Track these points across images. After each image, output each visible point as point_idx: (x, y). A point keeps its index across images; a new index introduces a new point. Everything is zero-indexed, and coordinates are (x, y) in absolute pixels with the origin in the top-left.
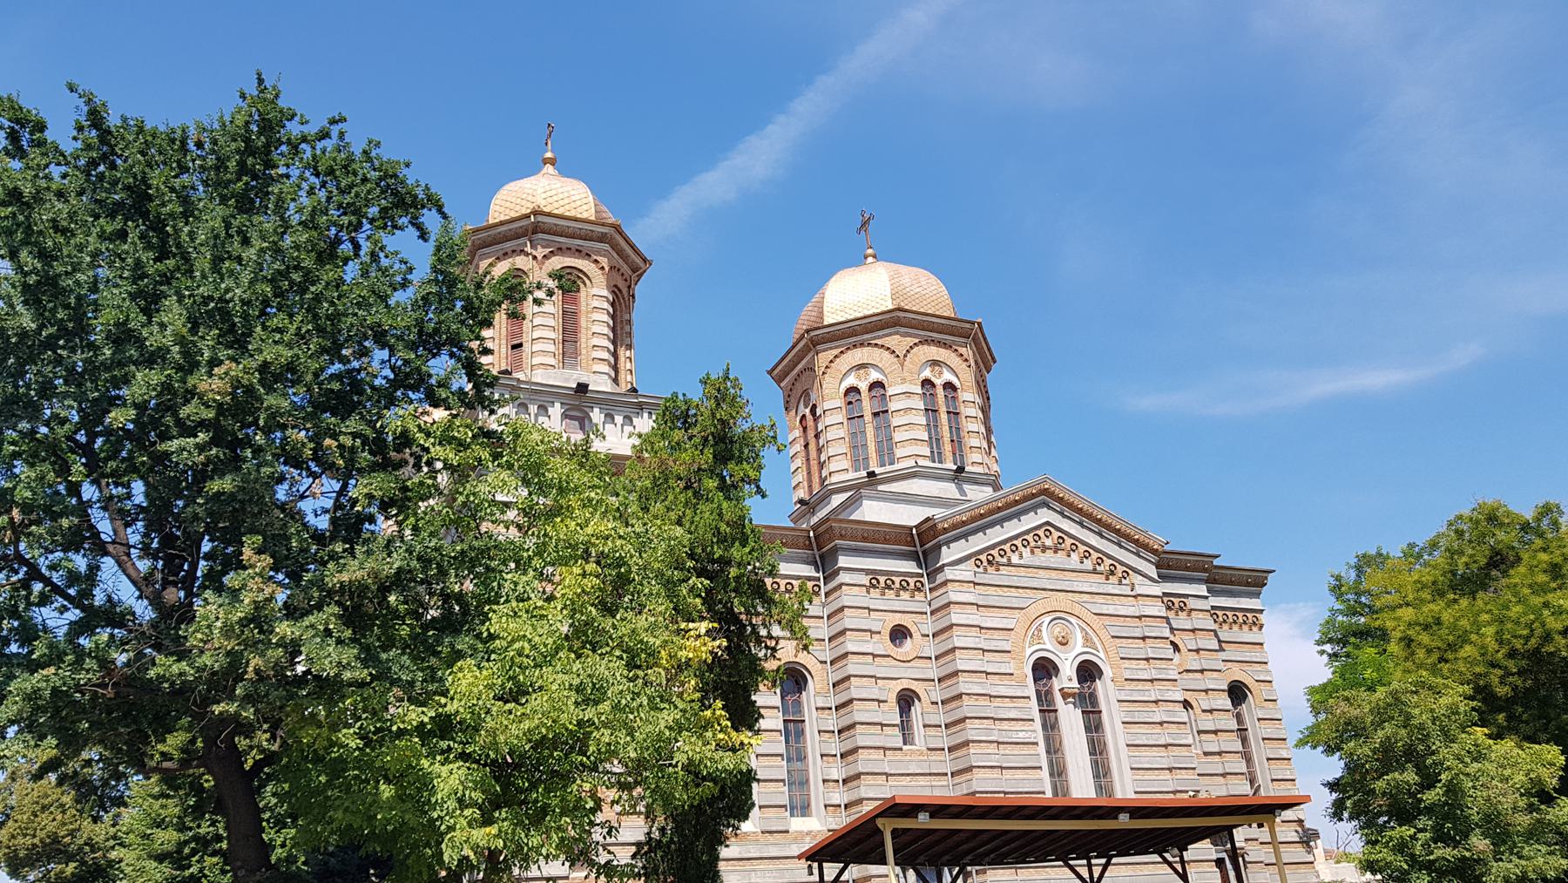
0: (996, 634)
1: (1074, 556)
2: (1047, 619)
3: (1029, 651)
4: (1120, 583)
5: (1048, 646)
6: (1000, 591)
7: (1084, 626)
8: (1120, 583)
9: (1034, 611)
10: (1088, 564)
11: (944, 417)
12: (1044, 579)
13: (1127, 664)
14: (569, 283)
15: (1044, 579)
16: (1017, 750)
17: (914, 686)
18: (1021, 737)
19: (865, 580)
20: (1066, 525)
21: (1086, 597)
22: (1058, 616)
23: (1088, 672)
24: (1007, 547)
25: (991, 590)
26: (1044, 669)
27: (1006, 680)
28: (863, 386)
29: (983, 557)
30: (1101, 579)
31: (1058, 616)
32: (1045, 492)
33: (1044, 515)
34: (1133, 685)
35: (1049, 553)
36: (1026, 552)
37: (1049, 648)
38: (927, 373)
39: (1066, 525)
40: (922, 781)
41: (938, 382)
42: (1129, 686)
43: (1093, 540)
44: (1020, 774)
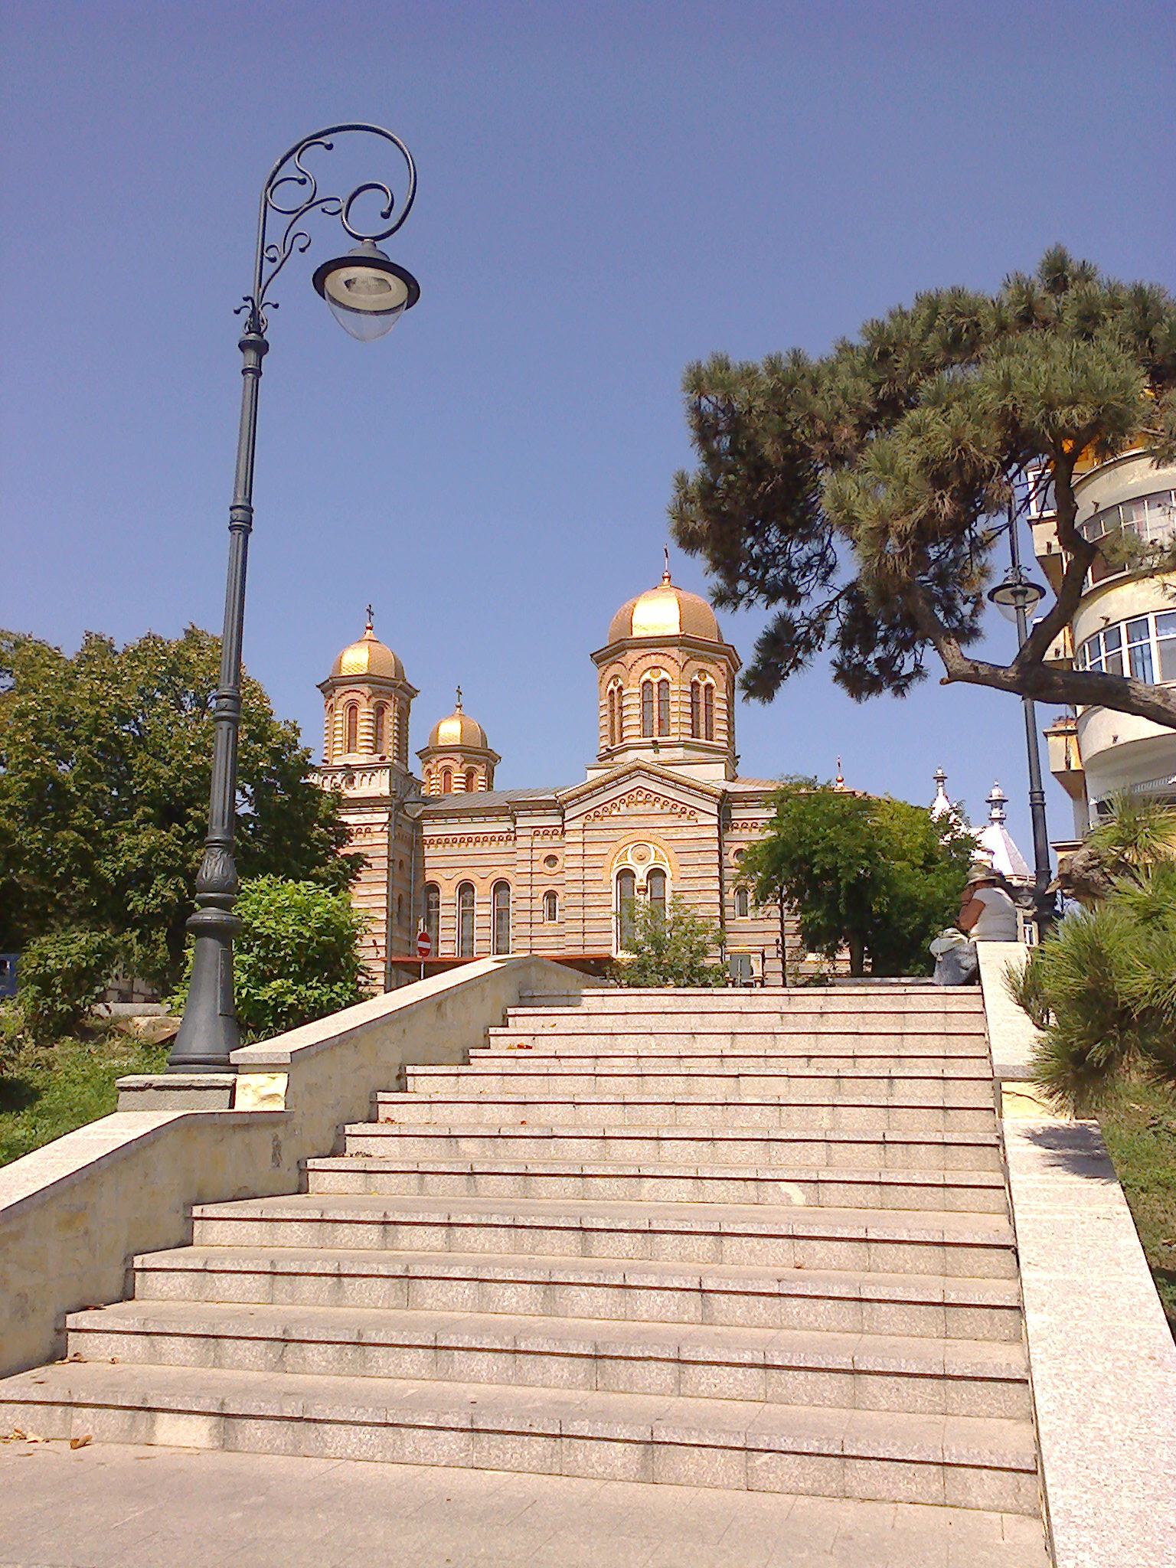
0: (595, 858)
1: (658, 805)
2: (631, 846)
3: (616, 865)
4: (689, 818)
5: (630, 861)
6: (602, 833)
7: (656, 848)
8: (689, 818)
9: (622, 842)
10: (667, 809)
11: (656, 705)
12: (633, 821)
13: (684, 869)
14: (353, 707)
15: (633, 821)
16: (597, 923)
17: (555, 888)
18: (602, 915)
19: (531, 832)
20: (653, 787)
21: (661, 830)
22: (638, 843)
23: (656, 873)
24: (608, 805)
25: (596, 833)
26: (626, 874)
27: (598, 884)
28: (616, 688)
29: (591, 814)
30: (675, 817)
31: (638, 843)
32: (638, 768)
33: (639, 782)
34: (686, 881)
35: (640, 806)
36: (623, 807)
37: (631, 862)
38: (647, 676)
39: (653, 787)
40: (553, 939)
41: (655, 680)
42: (682, 882)
43: (672, 794)
44: (597, 936)
